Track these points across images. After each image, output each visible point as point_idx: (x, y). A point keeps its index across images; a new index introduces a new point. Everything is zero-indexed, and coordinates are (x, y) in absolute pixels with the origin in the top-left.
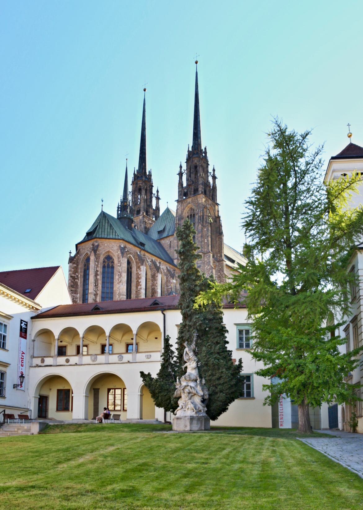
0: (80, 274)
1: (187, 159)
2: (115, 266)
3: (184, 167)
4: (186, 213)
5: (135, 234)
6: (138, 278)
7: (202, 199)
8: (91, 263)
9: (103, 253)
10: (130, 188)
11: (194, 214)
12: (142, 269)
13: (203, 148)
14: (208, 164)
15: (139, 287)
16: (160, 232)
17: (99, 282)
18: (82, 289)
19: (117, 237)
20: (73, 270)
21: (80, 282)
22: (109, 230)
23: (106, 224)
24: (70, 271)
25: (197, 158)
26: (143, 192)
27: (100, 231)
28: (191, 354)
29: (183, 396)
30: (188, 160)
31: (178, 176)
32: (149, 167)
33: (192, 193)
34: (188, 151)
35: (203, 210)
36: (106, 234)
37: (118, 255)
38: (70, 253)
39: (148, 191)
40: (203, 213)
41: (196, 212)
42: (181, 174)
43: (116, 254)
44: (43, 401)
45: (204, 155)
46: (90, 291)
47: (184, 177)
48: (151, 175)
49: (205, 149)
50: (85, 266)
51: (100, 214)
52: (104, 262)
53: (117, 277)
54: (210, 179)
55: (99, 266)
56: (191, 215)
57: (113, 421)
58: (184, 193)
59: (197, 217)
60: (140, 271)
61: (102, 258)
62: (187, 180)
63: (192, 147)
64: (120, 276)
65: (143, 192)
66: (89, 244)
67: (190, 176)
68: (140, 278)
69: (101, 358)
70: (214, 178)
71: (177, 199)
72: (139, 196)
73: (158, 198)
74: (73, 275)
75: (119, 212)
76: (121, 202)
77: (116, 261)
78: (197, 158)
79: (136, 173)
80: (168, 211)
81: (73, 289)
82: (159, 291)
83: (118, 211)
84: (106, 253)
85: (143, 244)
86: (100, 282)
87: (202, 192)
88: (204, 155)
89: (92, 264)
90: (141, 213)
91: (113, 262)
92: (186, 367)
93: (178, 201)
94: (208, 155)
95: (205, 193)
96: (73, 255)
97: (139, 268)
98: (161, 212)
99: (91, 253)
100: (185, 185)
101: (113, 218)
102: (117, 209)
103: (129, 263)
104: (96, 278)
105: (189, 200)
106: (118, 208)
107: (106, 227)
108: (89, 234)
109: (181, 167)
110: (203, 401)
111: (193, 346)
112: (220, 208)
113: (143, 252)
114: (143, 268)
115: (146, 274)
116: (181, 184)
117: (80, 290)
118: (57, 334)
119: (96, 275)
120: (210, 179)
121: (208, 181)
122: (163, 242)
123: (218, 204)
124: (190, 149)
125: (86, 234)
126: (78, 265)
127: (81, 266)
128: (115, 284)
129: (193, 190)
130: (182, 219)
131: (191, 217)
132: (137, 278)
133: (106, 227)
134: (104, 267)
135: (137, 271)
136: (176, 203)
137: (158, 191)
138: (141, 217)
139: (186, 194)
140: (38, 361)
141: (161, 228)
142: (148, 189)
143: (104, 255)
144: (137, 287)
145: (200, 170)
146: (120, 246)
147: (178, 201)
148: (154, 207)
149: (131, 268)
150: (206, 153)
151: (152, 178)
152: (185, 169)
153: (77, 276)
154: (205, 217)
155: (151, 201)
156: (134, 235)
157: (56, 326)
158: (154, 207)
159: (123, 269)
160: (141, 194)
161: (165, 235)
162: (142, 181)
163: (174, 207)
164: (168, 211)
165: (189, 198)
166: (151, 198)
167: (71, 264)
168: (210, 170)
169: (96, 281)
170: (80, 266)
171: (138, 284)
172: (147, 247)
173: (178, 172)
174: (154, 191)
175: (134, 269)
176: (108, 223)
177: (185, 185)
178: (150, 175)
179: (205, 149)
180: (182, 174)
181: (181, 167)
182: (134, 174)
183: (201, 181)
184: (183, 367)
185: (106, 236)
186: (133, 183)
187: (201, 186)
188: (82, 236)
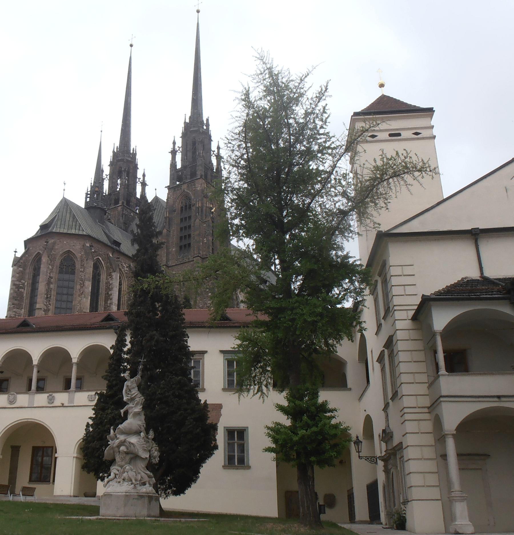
0: (27, 282)
1: (183, 133)
2: (76, 271)
3: (179, 143)
4: (178, 206)
5: (109, 230)
6: (109, 288)
7: (200, 185)
8: (42, 266)
9: (61, 253)
10: (107, 170)
12: (114, 277)
14: (210, 140)
15: (109, 302)
17: (52, 293)
18: (28, 301)
19: (81, 233)
20: (18, 275)
21: (26, 292)
22: (71, 223)
23: (68, 215)
24: (13, 276)
26: (124, 175)
27: (59, 223)
28: (135, 392)
29: (118, 458)
30: (184, 136)
31: (170, 156)
32: (134, 143)
33: (189, 177)
34: (185, 122)
35: (202, 200)
36: (66, 227)
38: (16, 252)
39: (131, 175)
40: (202, 203)
41: (193, 202)
42: (174, 153)
43: (78, 255)
45: (205, 127)
46: (38, 306)
48: (136, 153)
49: (207, 120)
50: (35, 269)
51: (61, 202)
52: (61, 264)
53: (78, 287)
55: (54, 270)
56: (186, 206)
57: (22, 498)
59: (194, 208)
60: (112, 279)
61: (58, 262)
63: (190, 117)
64: (83, 285)
65: (124, 175)
66: (43, 242)
67: (186, 155)
68: (111, 289)
69: (22, 399)
71: (168, 184)
72: (119, 181)
73: (144, 185)
74: (17, 283)
75: (88, 200)
76: (92, 187)
77: (78, 266)
79: (115, 151)
81: (16, 302)
83: (86, 198)
85: (118, 244)
86: (53, 293)
87: (201, 176)
88: (205, 127)
89: (43, 268)
90: (120, 202)
91: (74, 265)
92: (126, 413)
93: (169, 188)
94: (210, 129)
96: (19, 255)
97: (110, 275)
99: (43, 253)
100: (179, 166)
101: (78, 207)
102: (84, 196)
103: (96, 267)
104: (49, 288)
105: (184, 187)
106: (87, 194)
107: (68, 219)
108: (44, 227)
109: (174, 143)
110: (150, 466)
111: (139, 376)
113: (116, 255)
114: (116, 276)
115: (120, 284)
116: (173, 165)
117: (26, 302)
119: (49, 283)
121: (210, 162)
124: (188, 121)
125: (39, 228)
126: (24, 270)
127: (29, 271)
128: (74, 296)
129: (189, 174)
130: (175, 211)
131: (186, 209)
132: (106, 290)
133: (68, 219)
134: (61, 272)
135: (107, 279)
136: (166, 191)
137: (144, 175)
138: (120, 208)
139: (180, 179)
142: (131, 171)
143: (61, 255)
144: (106, 301)
145: (199, 147)
147: (169, 188)
148: (138, 196)
149: (99, 275)
150: (208, 125)
151: (137, 157)
152: (180, 146)
153: (23, 284)
154: (204, 208)
155: (135, 189)
156: (107, 231)
158: (138, 196)
159: (87, 276)
160: (121, 178)
163: (163, 196)
165: (184, 183)
166: (135, 183)
167: (15, 267)
169: (48, 291)
170: (27, 271)
171: (108, 297)
173: (170, 150)
174: (139, 175)
175: (103, 277)
176: (70, 213)
177: (179, 166)
178: (134, 155)
179: (207, 120)
180: (177, 151)
181: (174, 143)
183: (199, 162)
184: (122, 411)
185: (65, 231)
186: (112, 164)
187: (200, 168)
188: (33, 231)
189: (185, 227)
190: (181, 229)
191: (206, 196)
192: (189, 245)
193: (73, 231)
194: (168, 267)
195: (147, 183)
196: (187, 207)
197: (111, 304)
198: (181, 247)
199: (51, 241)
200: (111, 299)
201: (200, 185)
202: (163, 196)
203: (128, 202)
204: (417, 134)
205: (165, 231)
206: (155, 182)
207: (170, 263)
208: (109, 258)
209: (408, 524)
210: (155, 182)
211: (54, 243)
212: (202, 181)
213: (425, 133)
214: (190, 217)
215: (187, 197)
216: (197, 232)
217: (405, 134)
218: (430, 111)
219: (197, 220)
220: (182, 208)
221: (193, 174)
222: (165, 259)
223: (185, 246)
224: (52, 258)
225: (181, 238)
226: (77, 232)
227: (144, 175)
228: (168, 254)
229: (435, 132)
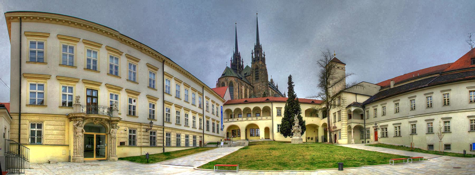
4: (254, 68)
6: (241, 90)
7: (261, 63)
25: (258, 49)
44: (228, 133)
47: (254, 55)
54: (263, 56)
58: (254, 61)
62: (255, 56)
70: (264, 55)
73: (243, 62)
78: (258, 49)
80: (247, 66)
95: (261, 60)
112: (267, 66)
116: (252, 57)
118: (233, 111)
120: (263, 56)
140: (226, 120)
141: (245, 73)
157: (233, 108)
163: (250, 65)
164: (247, 66)
171: (241, 92)
174: (241, 60)
175: (240, 87)
196: (257, 68)
202: (250, 65)
206: (247, 62)
209: (417, 132)
210: (247, 62)
215: (257, 66)
221: (258, 60)
224: (227, 83)
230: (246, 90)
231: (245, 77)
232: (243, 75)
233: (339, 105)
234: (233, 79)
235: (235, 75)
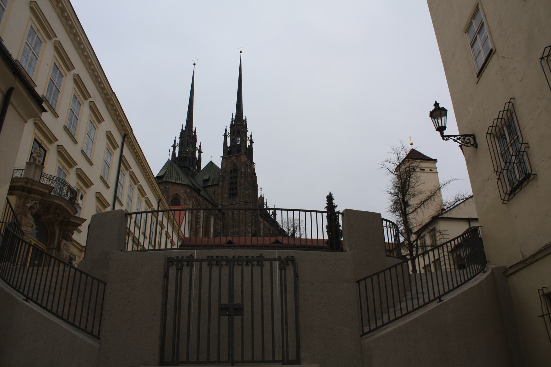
7: (243, 158)
11: (236, 170)
13: (244, 118)
15: (198, 226)
16: (206, 181)
19: (183, 183)
32: (195, 125)
34: (232, 118)
37: (184, 198)
42: (225, 136)
43: (182, 197)
47: (228, 139)
51: (168, 162)
54: (248, 143)
56: (234, 170)
58: (228, 152)
59: (239, 172)
61: (170, 200)
70: (251, 142)
73: (200, 152)
80: (211, 164)
82: (212, 230)
84: (174, 195)
95: (245, 153)
98: (203, 165)
100: (229, 145)
105: (233, 158)
109: (226, 130)
116: (225, 143)
120: (248, 143)
122: (208, 189)
123: (254, 163)
124: (234, 117)
136: (221, 159)
137: (200, 146)
141: (206, 177)
144: (196, 226)
146: (186, 191)
161: (210, 184)
162: (188, 137)
163: (218, 163)
164: (211, 164)
165: (233, 156)
168: (249, 135)
172: (202, 193)
174: (198, 146)
176: (175, 170)
177: (229, 145)
181: (226, 130)
182: (182, 129)
185: (174, 181)
189: (233, 183)
190: (231, 183)
191: (247, 166)
192: (236, 194)
193: (178, 182)
194: (221, 205)
195: (202, 151)
197: (200, 227)
198: (230, 194)
199: (167, 187)
200: (200, 224)
201: (243, 158)
202: (218, 163)
203: (193, 162)
204: (431, 170)
205: (221, 184)
207: (224, 204)
208: (197, 199)
211: (168, 188)
212: (244, 156)
213: (434, 170)
214: (236, 177)
216: (242, 187)
217: (426, 170)
218: (435, 161)
219: (243, 180)
220: (231, 171)
221: (239, 151)
222: (220, 201)
223: (233, 194)
225: (230, 189)
226: (181, 182)
227: (200, 146)
228: (222, 198)
229: (438, 170)
230: (207, 219)
231: (205, 187)
232: (201, 184)
233: (435, 247)
234: (181, 191)
235: (186, 181)
